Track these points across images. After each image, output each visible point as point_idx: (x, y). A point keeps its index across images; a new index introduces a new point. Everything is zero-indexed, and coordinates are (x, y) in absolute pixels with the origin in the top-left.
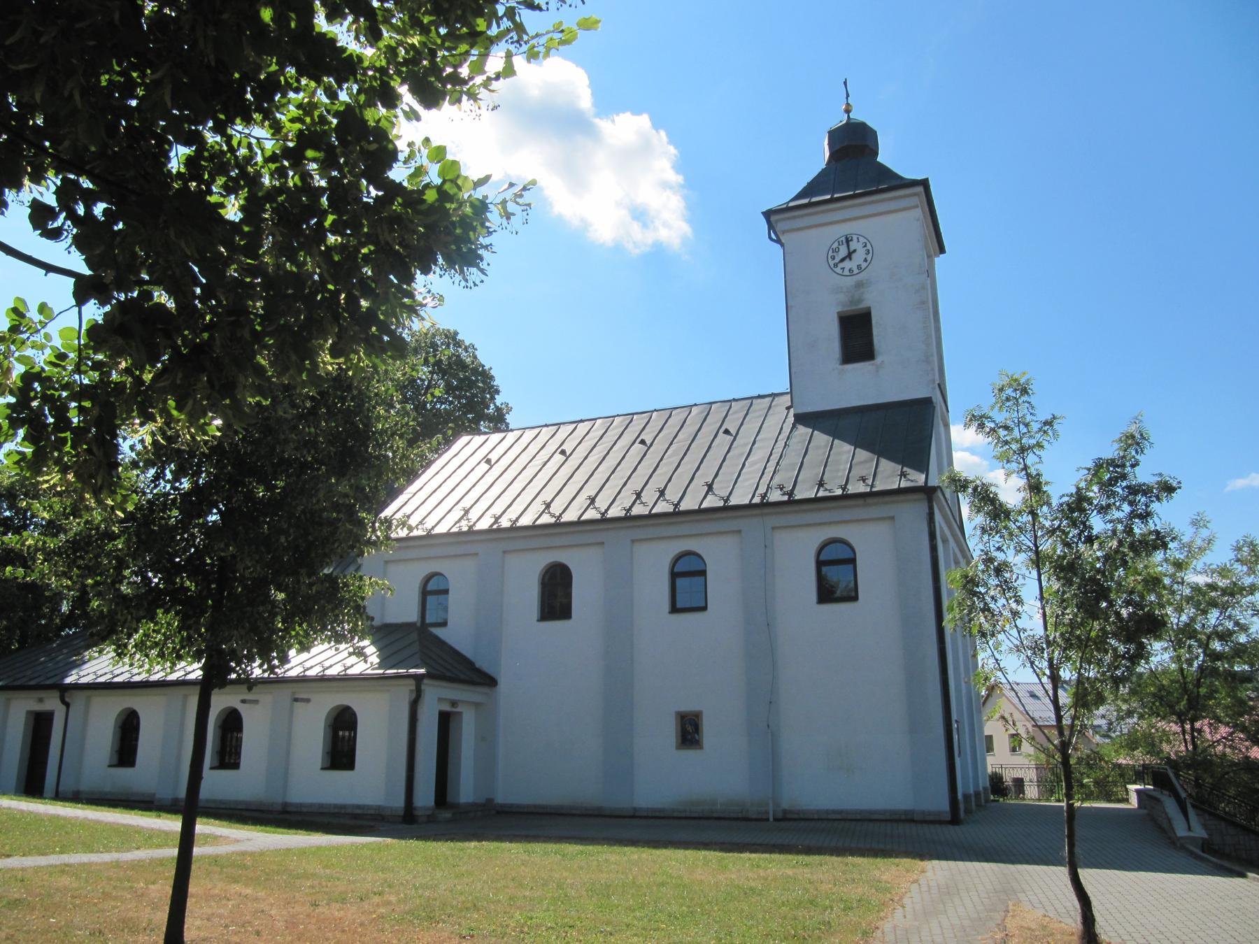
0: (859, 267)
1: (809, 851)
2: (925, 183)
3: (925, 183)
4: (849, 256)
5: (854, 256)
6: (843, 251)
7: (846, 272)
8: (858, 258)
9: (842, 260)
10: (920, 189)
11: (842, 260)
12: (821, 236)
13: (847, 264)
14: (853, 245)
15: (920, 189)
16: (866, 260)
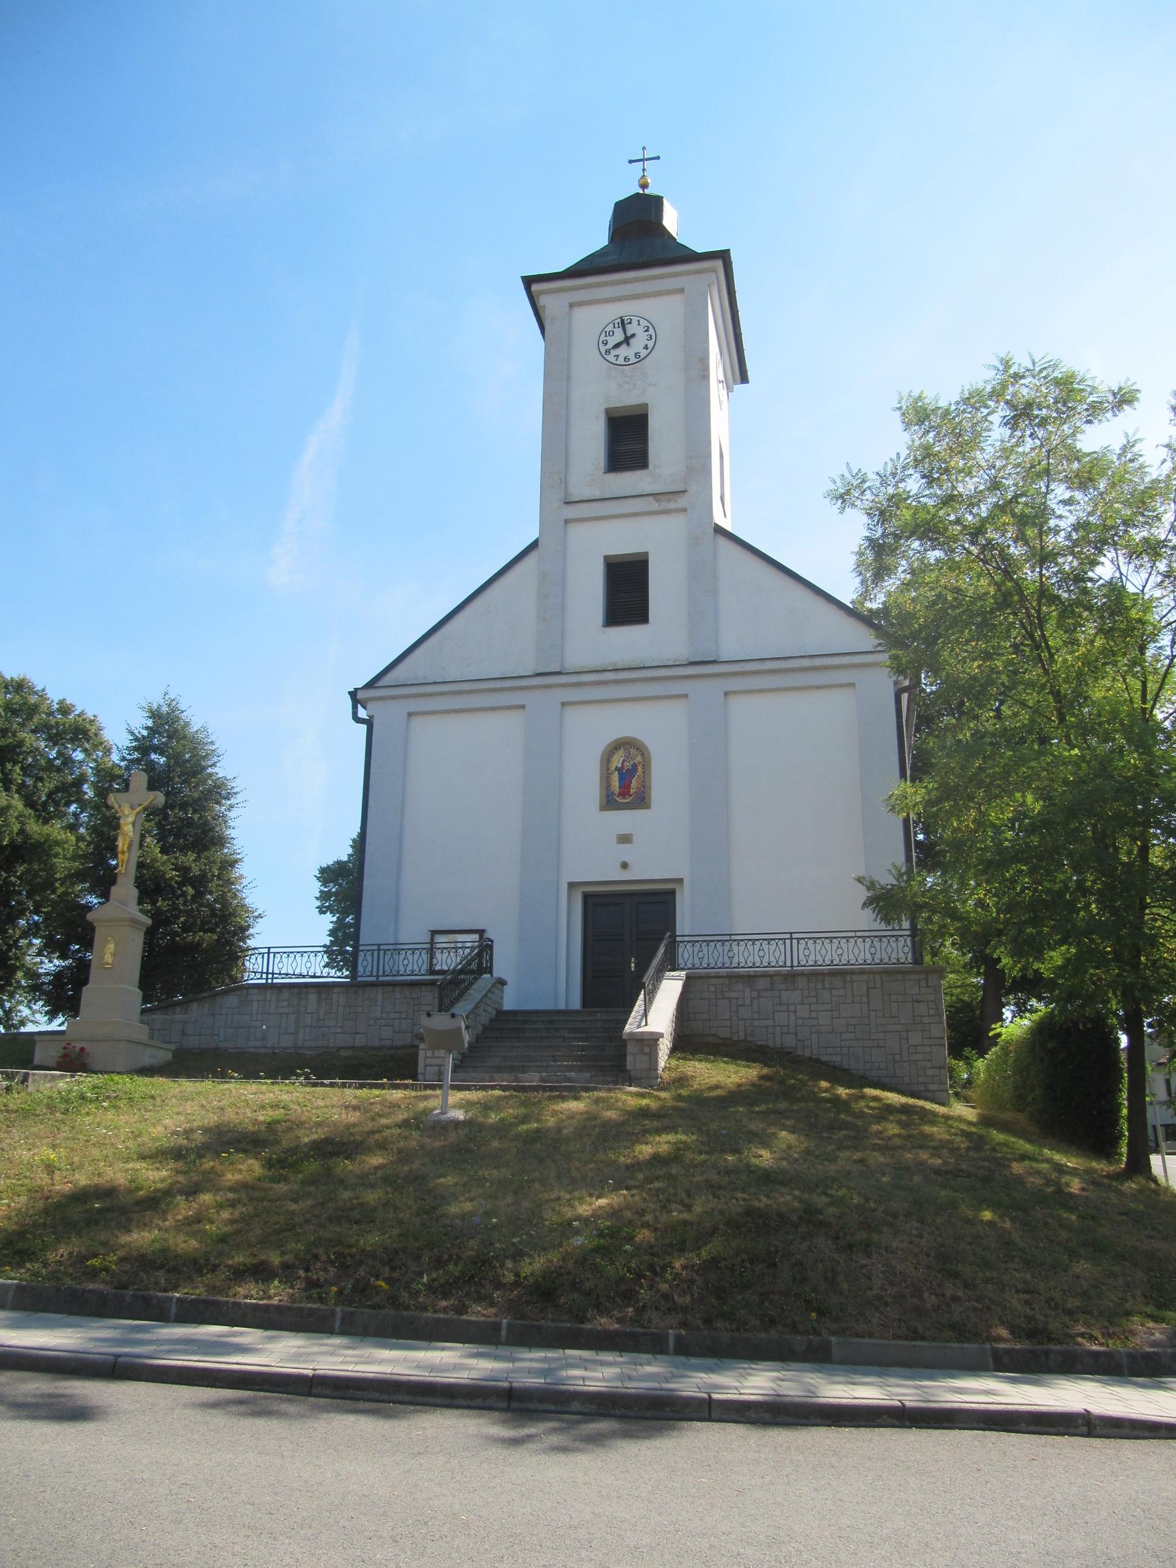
0: (637, 355)
1: (1108, 1437)
2: (724, 256)
3: (724, 256)
4: (627, 340)
5: (632, 341)
6: (619, 336)
7: (621, 361)
8: (638, 344)
9: (617, 346)
10: (718, 264)
11: (617, 346)
12: (592, 318)
13: (623, 351)
14: (630, 330)
15: (718, 264)
16: (646, 347)
